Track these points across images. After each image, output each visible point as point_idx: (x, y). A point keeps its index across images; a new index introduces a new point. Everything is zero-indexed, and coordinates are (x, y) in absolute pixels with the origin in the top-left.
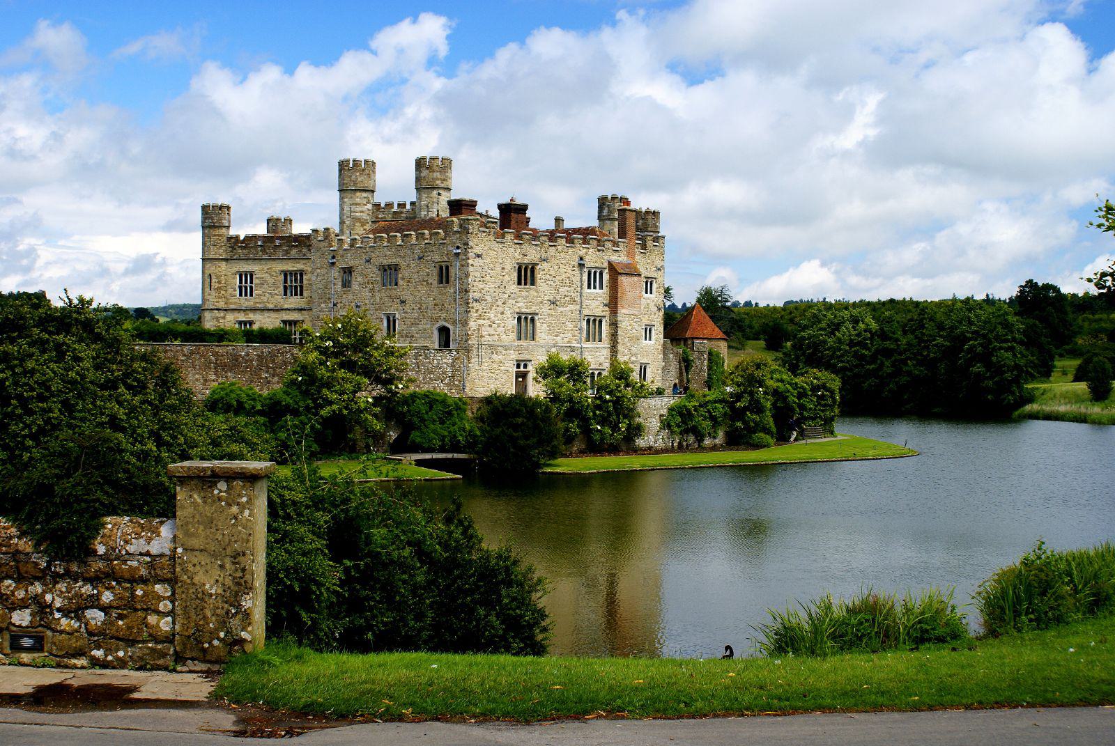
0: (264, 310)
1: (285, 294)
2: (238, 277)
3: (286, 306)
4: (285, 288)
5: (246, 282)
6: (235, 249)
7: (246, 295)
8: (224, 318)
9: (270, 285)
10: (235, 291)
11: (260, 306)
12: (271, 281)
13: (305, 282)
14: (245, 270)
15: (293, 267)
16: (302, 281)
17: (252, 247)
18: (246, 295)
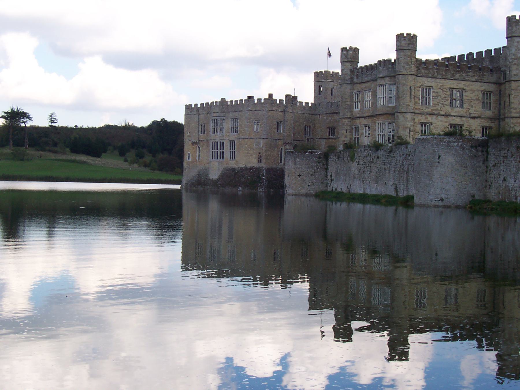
0: (438, 115)
2: (421, 89)
3: (452, 114)
4: (452, 100)
6: (419, 69)
10: (420, 100)
11: (435, 112)
12: (442, 94)
13: (464, 97)
15: (457, 86)
16: (461, 96)
17: (431, 69)
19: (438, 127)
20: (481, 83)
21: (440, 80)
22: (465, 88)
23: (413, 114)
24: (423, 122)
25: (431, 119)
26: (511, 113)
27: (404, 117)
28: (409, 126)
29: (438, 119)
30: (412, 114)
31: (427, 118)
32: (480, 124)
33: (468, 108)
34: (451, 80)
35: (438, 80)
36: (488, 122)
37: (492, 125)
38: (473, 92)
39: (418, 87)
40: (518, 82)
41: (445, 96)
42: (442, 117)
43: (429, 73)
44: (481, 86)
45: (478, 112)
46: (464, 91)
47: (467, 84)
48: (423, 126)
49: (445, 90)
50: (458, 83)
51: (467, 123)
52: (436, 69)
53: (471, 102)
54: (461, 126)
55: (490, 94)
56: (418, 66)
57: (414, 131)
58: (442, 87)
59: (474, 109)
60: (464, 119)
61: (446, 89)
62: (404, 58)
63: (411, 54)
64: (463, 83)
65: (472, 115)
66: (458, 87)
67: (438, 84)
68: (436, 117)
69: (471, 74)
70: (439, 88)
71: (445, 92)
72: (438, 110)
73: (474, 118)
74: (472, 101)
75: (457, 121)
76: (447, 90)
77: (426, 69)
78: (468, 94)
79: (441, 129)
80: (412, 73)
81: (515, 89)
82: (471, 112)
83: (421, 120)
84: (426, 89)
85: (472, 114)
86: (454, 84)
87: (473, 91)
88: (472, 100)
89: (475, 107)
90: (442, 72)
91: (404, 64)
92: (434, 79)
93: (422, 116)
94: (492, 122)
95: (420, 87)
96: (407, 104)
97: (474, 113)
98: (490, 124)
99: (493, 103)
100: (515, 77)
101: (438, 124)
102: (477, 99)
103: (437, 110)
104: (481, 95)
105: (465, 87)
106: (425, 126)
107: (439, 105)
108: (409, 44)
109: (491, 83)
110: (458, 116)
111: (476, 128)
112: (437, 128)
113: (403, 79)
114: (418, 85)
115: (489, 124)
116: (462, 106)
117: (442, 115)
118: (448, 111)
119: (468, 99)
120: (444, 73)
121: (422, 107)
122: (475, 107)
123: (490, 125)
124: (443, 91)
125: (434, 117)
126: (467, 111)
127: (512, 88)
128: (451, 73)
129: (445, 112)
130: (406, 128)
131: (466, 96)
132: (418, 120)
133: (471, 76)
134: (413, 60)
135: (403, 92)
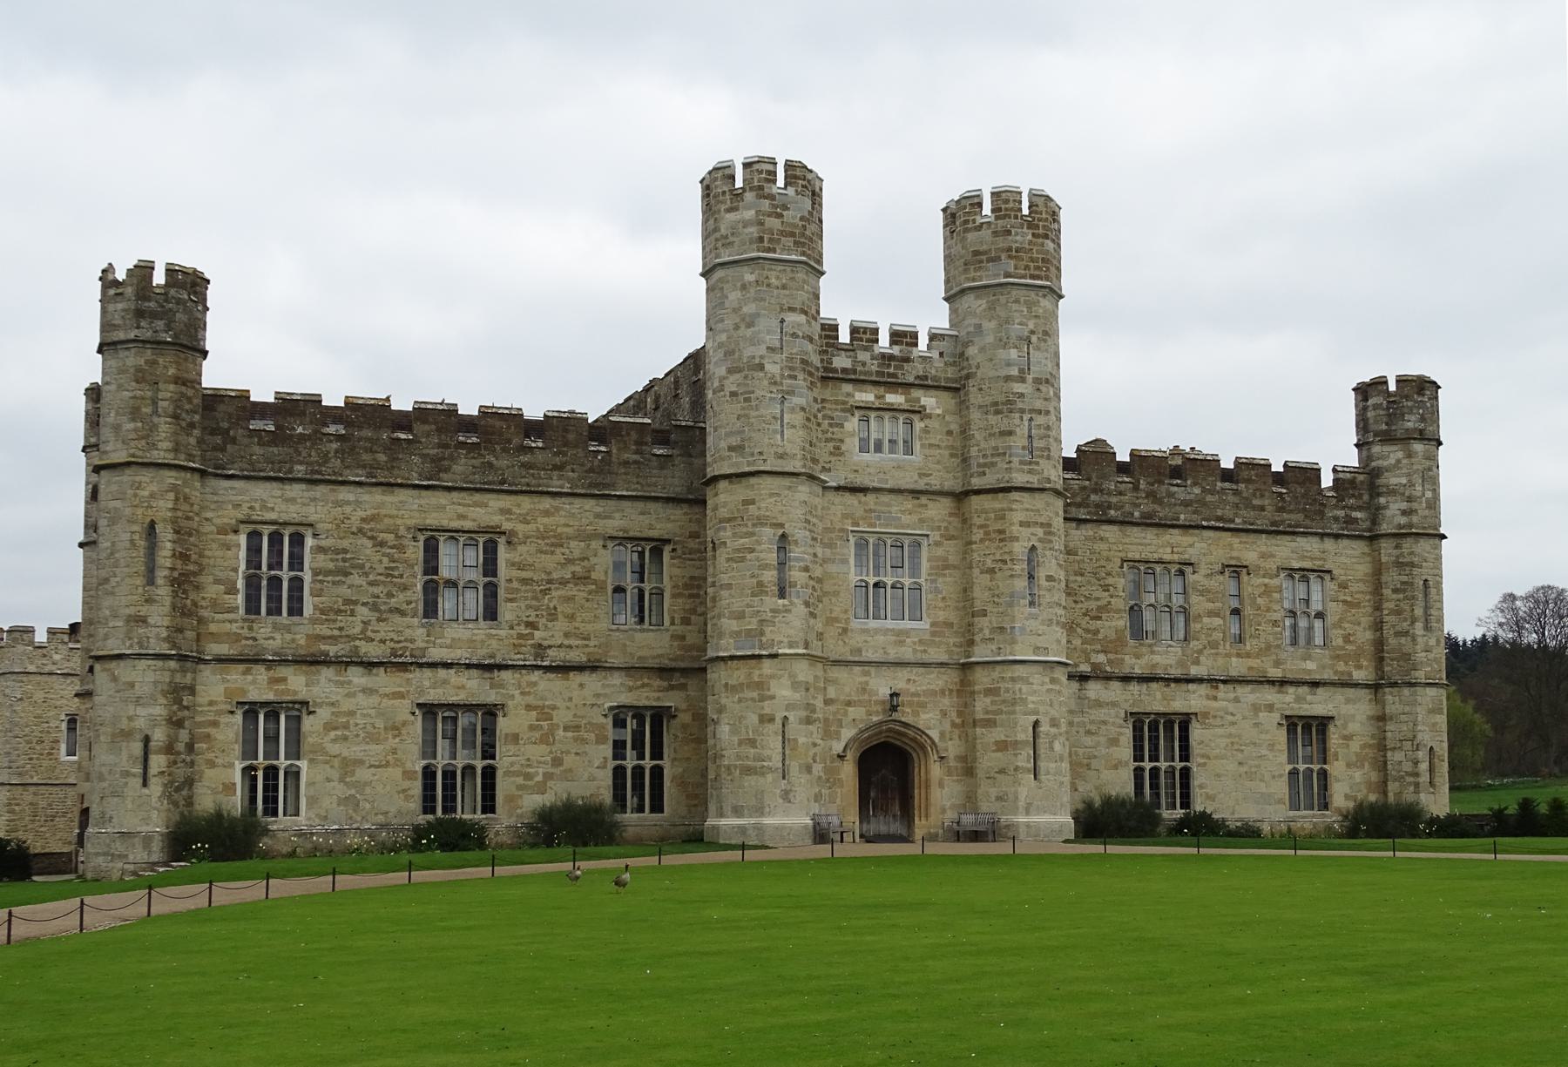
0: (348, 664)
1: (431, 610)
2: (243, 539)
3: (436, 654)
4: (431, 590)
5: (276, 564)
6: (234, 441)
7: (274, 610)
8: (192, 690)
9: (371, 577)
10: (232, 590)
11: (333, 650)
14: (272, 516)
15: (462, 517)
16: (490, 567)
18: (274, 610)
19: (348, 722)
20: (602, 502)
21: (360, 490)
22: (507, 526)
23: (172, 664)
24: (254, 703)
25: (307, 685)
26: (721, 635)
27: (115, 679)
28: (140, 723)
29: (349, 682)
30: (160, 663)
31: (284, 680)
32: (598, 696)
33: (530, 619)
34: (424, 493)
35: (345, 494)
36: (643, 686)
37: (671, 700)
38: (553, 545)
39: (222, 531)
40: (743, 480)
41: (386, 568)
42: (375, 671)
43: (292, 461)
44: (598, 516)
45: (587, 642)
46: (502, 541)
47: (519, 505)
48: (261, 718)
49: (390, 537)
50: (464, 505)
51: (522, 693)
52: (332, 438)
53: (545, 592)
54: (490, 712)
55: (657, 553)
56: (225, 425)
57: (180, 747)
58: (372, 525)
59: (561, 625)
60: (506, 675)
61: (394, 531)
62: (120, 387)
63: (153, 363)
64: (496, 502)
65: (554, 656)
66: (468, 525)
67: (348, 509)
68: (338, 673)
69: (540, 457)
70: (354, 529)
71: (392, 548)
72: (347, 636)
73: (564, 669)
74: (553, 586)
75: (463, 687)
76: (405, 542)
77: (277, 438)
78: (523, 552)
79: (369, 727)
80: (157, 456)
81: (736, 518)
82: (545, 643)
83: (244, 692)
84: (276, 539)
85: (550, 652)
86: (444, 507)
87: (559, 542)
88: (550, 582)
89: (572, 617)
90: (366, 450)
91: (117, 414)
92: (321, 490)
93: (247, 672)
94: (671, 688)
95: (236, 532)
96: (131, 611)
97: (560, 646)
98: (660, 694)
99: (674, 596)
100: (735, 458)
101: (345, 707)
102: (582, 579)
103: (341, 637)
104: (603, 561)
105: (507, 519)
106: (273, 716)
107: (352, 611)
108: (140, 314)
109: (668, 500)
110: (469, 666)
111: (575, 715)
112: (346, 727)
113: (114, 488)
114: (229, 516)
115: (656, 695)
116: (491, 613)
117: (370, 665)
118: (412, 641)
119: (524, 581)
120: (382, 457)
121: (251, 629)
122: (572, 617)
123: (658, 699)
124: (374, 546)
125: (327, 673)
126: (520, 636)
127: (723, 512)
128: (424, 456)
129: (392, 645)
130: (127, 735)
131: (513, 564)
132: (228, 693)
133: (544, 469)
134: (168, 391)
135: (112, 554)
